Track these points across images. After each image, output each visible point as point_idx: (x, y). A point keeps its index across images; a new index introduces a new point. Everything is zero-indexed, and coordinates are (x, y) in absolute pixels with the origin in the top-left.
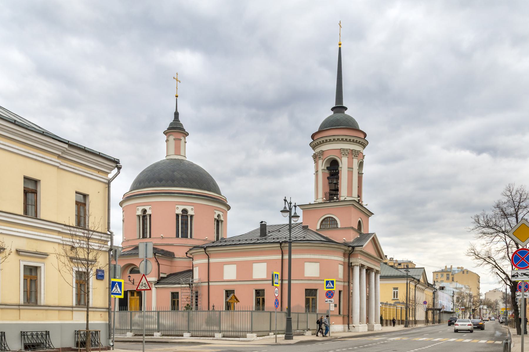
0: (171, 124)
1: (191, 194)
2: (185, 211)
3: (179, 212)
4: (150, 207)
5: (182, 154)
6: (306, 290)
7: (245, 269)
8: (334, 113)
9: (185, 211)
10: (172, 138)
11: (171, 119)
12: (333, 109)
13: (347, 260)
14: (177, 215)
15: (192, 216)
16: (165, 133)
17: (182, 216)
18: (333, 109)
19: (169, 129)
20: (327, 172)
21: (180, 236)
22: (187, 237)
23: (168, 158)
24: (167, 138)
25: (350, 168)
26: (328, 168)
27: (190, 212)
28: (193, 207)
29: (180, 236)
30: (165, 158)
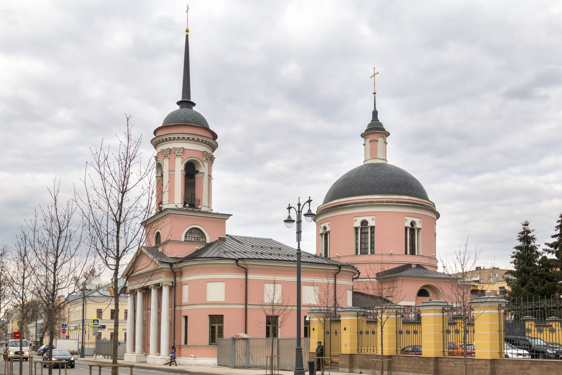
0: (369, 125)
2: (364, 223)
3: (358, 224)
4: (329, 223)
5: (380, 155)
8: (181, 108)
9: (364, 223)
10: (368, 140)
11: (369, 119)
12: (178, 103)
14: (356, 229)
15: (372, 228)
16: (363, 136)
17: (361, 229)
18: (178, 103)
19: (367, 131)
21: (359, 253)
22: (367, 253)
23: (366, 163)
24: (365, 140)
27: (371, 223)
28: (374, 217)
29: (359, 253)
30: (363, 164)
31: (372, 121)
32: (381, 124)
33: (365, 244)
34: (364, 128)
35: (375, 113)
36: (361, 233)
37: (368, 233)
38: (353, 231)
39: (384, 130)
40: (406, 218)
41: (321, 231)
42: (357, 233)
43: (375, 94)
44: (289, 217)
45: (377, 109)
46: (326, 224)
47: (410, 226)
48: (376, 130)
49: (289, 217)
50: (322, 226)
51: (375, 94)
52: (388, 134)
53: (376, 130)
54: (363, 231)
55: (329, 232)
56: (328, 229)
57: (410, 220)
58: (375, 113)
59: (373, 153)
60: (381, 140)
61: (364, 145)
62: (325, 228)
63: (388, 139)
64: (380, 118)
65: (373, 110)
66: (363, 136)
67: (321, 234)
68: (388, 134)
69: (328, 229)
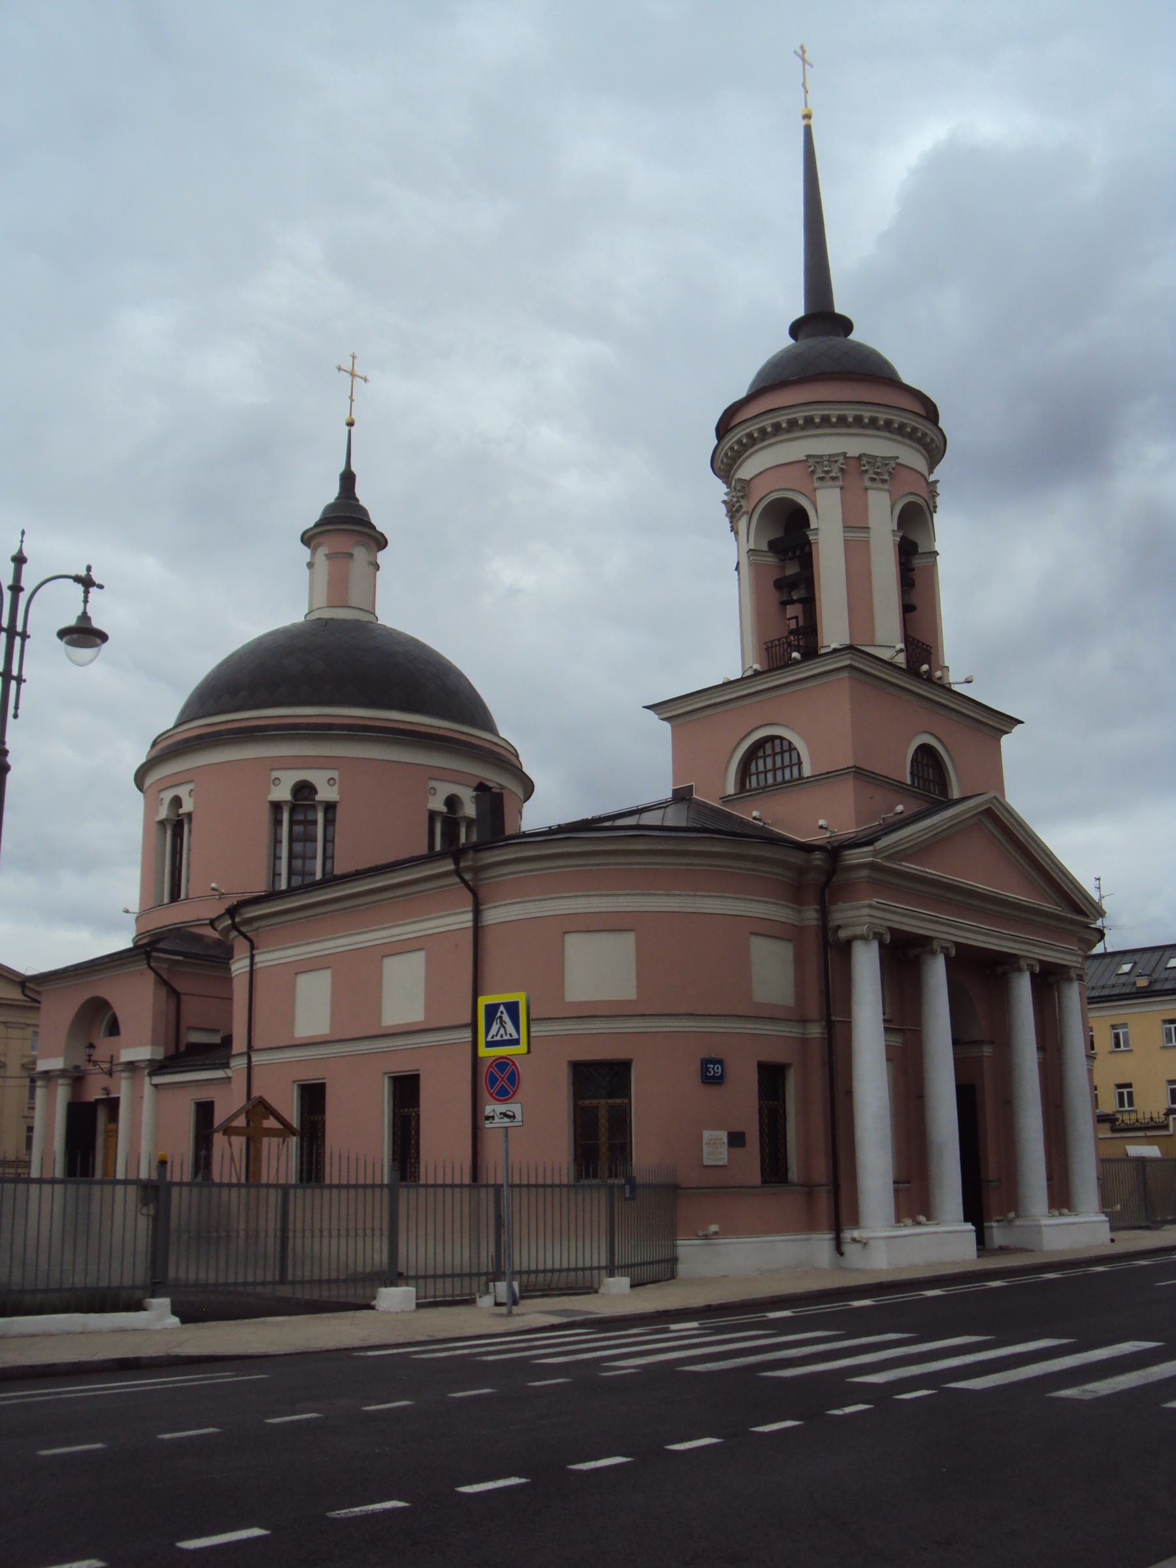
0: (330, 508)
1: (331, 727)
2: (304, 790)
3: (283, 793)
4: (191, 786)
5: (355, 598)
6: (570, 1062)
7: (357, 983)
9: (304, 790)
10: (322, 551)
11: (331, 492)
13: (811, 915)
14: (276, 806)
15: (330, 807)
16: (308, 539)
17: (293, 809)
19: (317, 525)
20: (771, 559)
23: (310, 617)
24: (313, 554)
25: (856, 529)
26: (773, 546)
27: (326, 793)
28: (335, 774)
31: (337, 499)
32: (363, 511)
33: (304, 858)
34: (313, 515)
35: (348, 479)
36: (292, 822)
37: (315, 822)
38: (266, 816)
39: (373, 527)
40: (432, 784)
41: (163, 813)
42: (277, 822)
43: (351, 424)
44: (85, 617)
45: (353, 469)
46: (183, 791)
47: (444, 809)
48: (346, 526)
49: (85, 617)
50: (168, 796)
51: (351, 424)
52: (381, 542)
53: (346, 526)
54: (300, 817)
55: (189, 815)
56: (187, 806)
57: (445, 789)
58: (348, 479)
59: (338, 588)
60: (360, 554)
61: (310, 565)
62: (177, 802)
63: (382, 557)
64: (362, 492)
65: (341, 468)
66: (308, 539)
67: (162, 823)
68: (381, 542)
69: (187, 806)
